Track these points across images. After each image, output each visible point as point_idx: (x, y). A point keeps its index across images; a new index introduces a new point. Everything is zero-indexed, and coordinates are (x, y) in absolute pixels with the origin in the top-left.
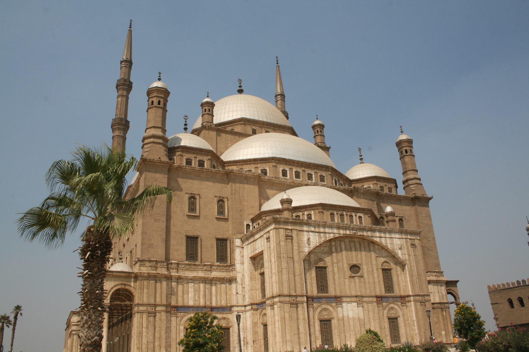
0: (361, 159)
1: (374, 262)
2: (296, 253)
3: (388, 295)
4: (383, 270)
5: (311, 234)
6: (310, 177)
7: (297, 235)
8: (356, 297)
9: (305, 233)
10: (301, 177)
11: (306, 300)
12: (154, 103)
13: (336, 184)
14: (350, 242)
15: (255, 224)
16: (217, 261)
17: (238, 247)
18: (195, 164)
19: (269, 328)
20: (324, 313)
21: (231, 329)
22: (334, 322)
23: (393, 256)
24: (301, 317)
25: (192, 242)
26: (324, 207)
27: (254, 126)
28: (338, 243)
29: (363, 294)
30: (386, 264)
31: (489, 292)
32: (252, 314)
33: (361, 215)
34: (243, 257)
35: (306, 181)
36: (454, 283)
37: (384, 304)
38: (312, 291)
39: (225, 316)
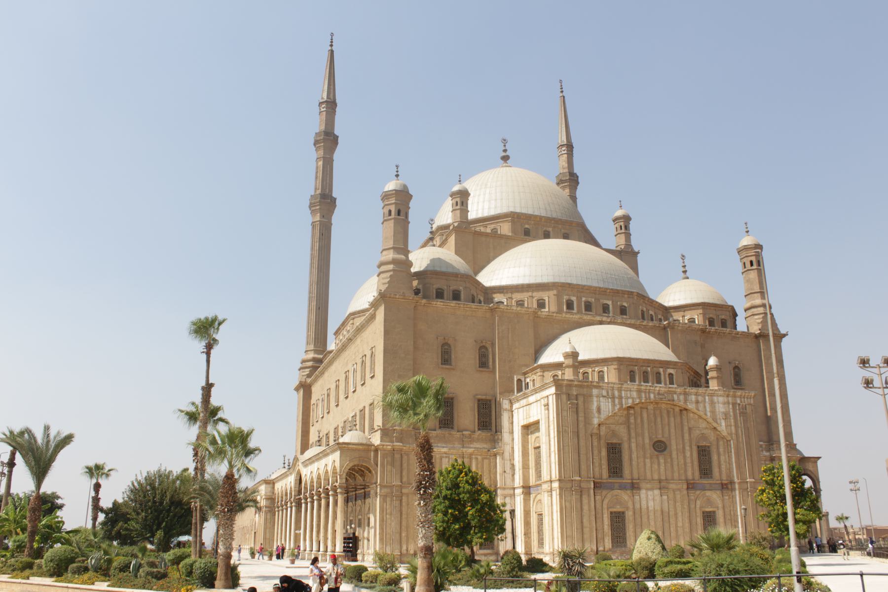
0: (685, 272)
1: (686, 436)
2: (581, 425)
4: (698, 447)
6: (605, 309)
7: (584, 402)
11: (592, 486)
12: (393, 213)
13: (643, 318)
14: (655, 409)
16: (479, 429)
17: (506, 410)
19: (546, 520)
22: (629, 515)
24: (586, 507)
26: (620, 362)
32: (524, 499)
34: (512, 423)
35: (600, 315)
37: (698, 492)
38: (601, 475)
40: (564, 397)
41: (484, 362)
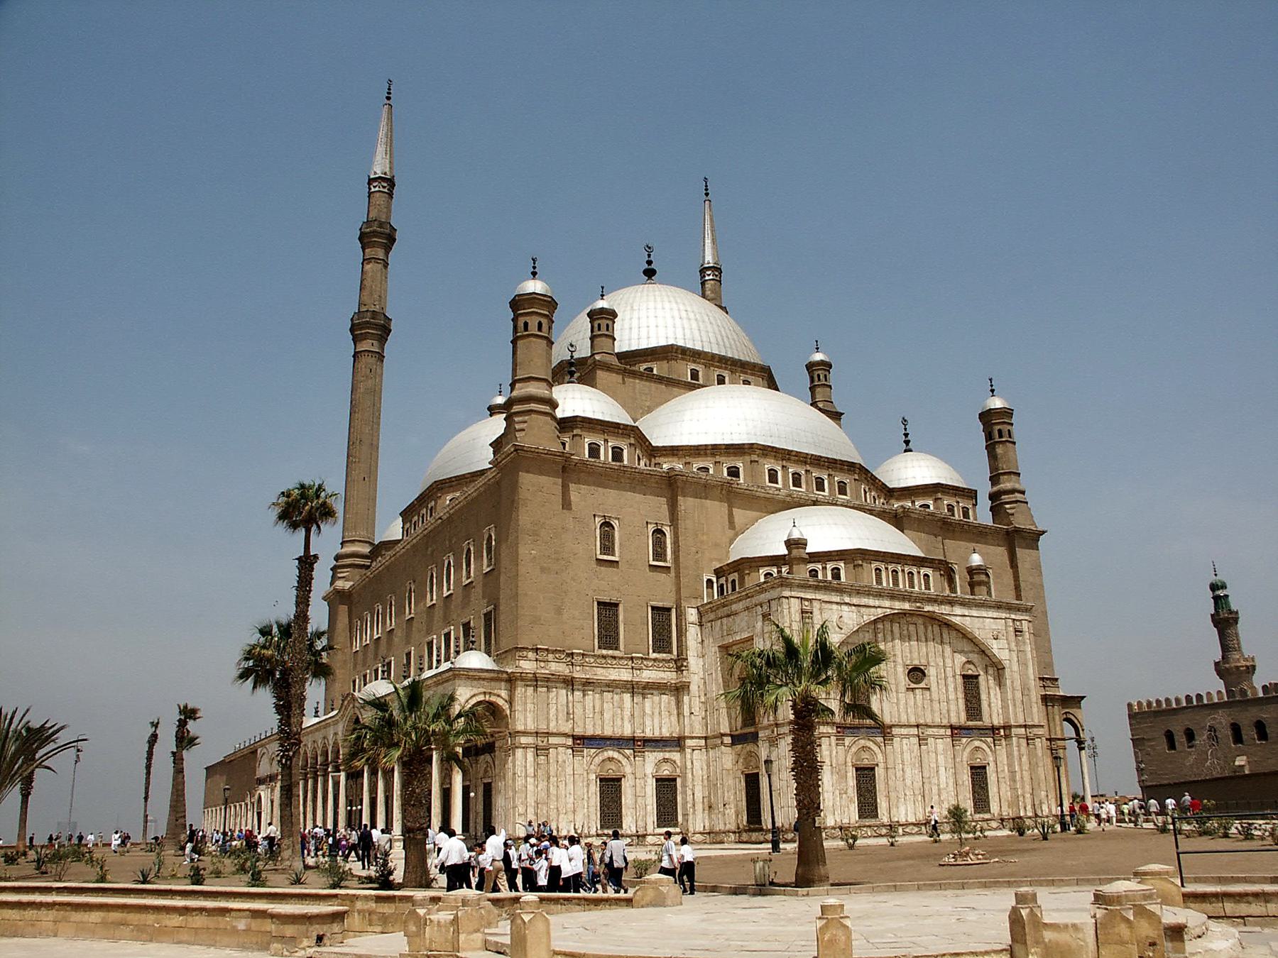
0: (907, 442)
3: (971, 726)
4: (964, 677)
5: (845, 608)
6: (820, 486)
8: (918, 726)
9: (835, 607)
10: (804, 485)
15: (723, 580)
18: (605, 455)
20: (865, 755)
21: (679, 780)
22: (879, 772)
23: (983, 652)
25: (608, 609)
27: (694, 362)
28: (888, 625)
29: (929, 721)
30: (971, 666)
31: (1130, 716)
33: (929, 572)
36: (1076, 701)
39: (667, 755)
40: (795, 604)
41: (659, 555)
